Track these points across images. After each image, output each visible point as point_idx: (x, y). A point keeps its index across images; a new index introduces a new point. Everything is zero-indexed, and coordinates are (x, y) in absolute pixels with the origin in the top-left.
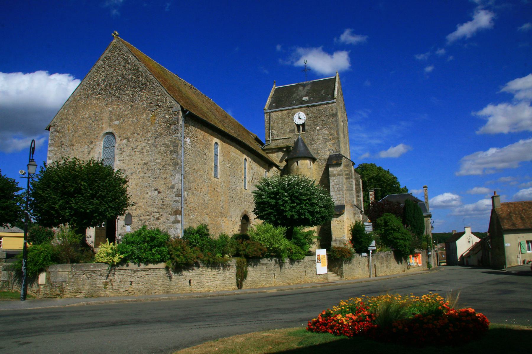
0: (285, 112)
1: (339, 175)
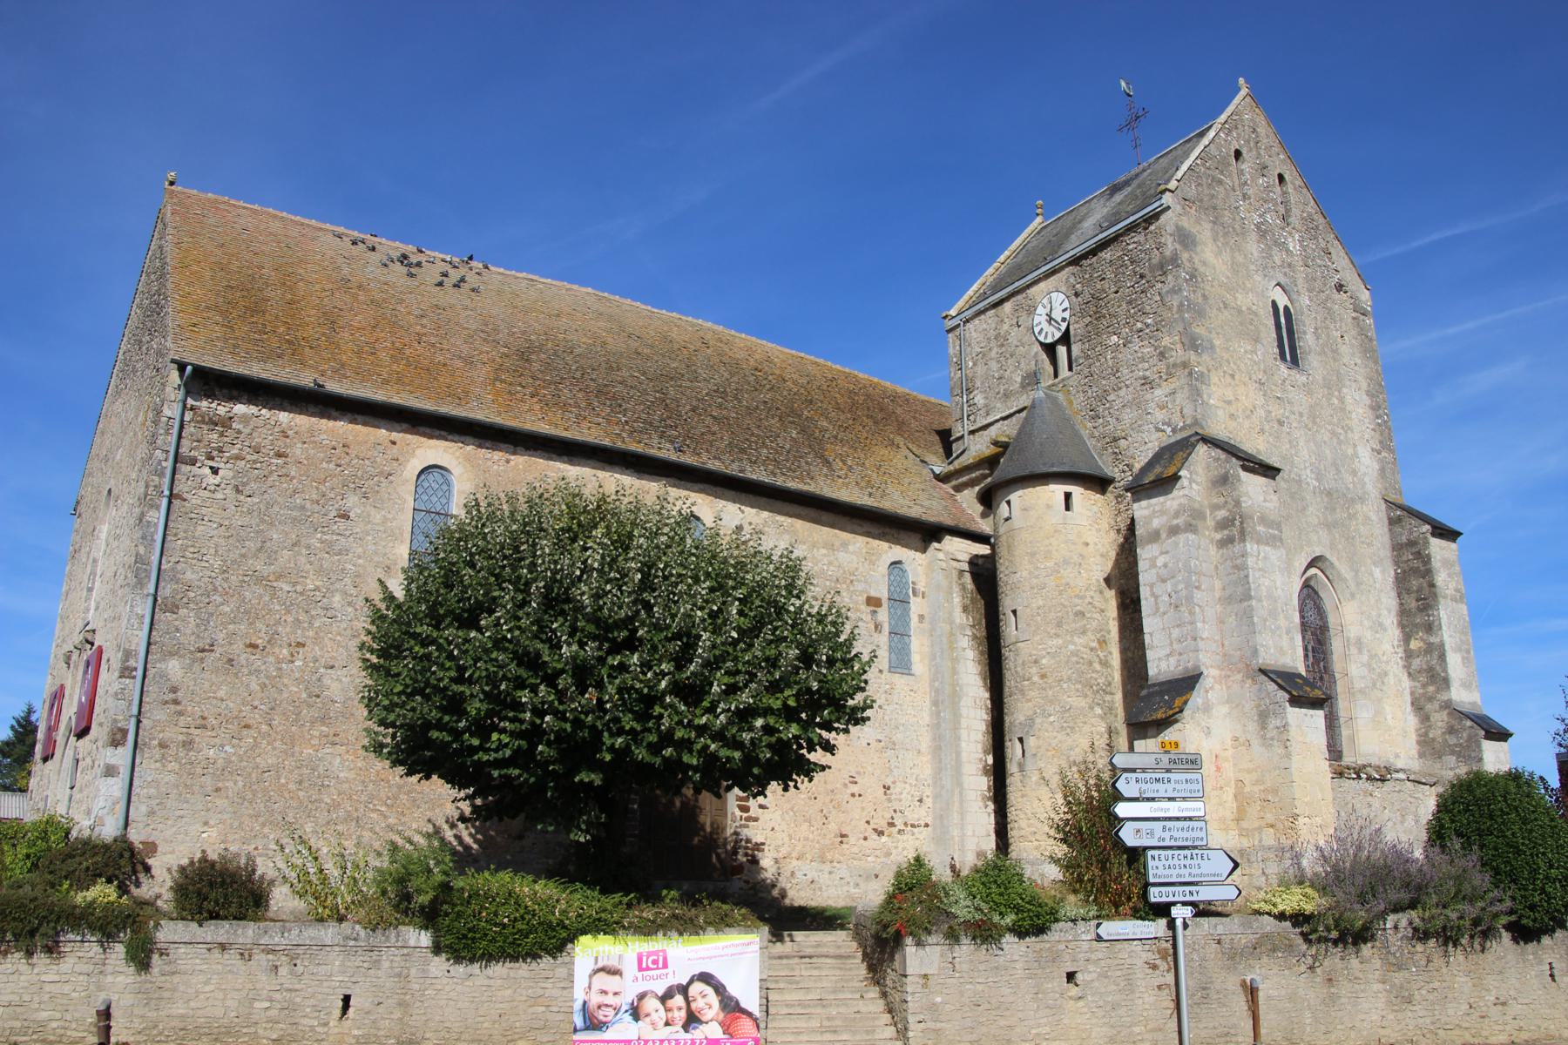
0: (1008, 306)
1: (1174, 531)
